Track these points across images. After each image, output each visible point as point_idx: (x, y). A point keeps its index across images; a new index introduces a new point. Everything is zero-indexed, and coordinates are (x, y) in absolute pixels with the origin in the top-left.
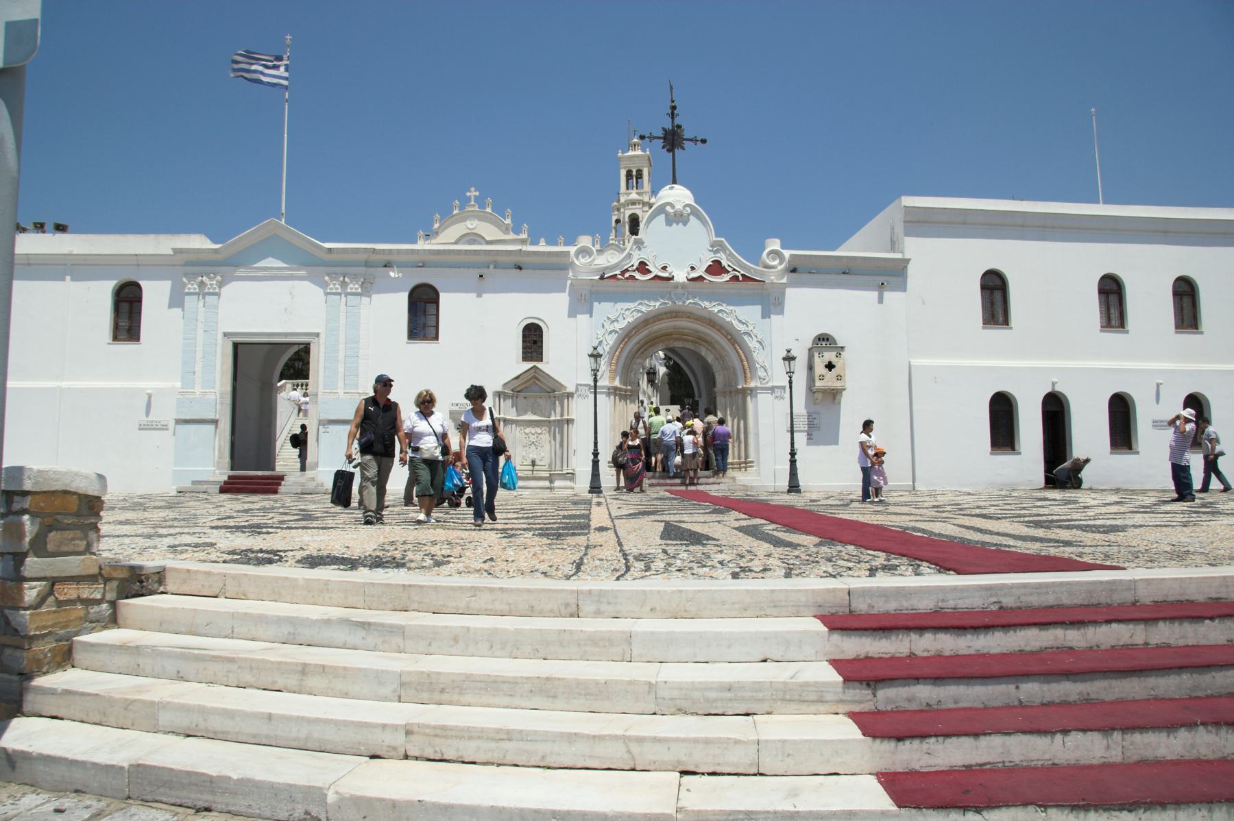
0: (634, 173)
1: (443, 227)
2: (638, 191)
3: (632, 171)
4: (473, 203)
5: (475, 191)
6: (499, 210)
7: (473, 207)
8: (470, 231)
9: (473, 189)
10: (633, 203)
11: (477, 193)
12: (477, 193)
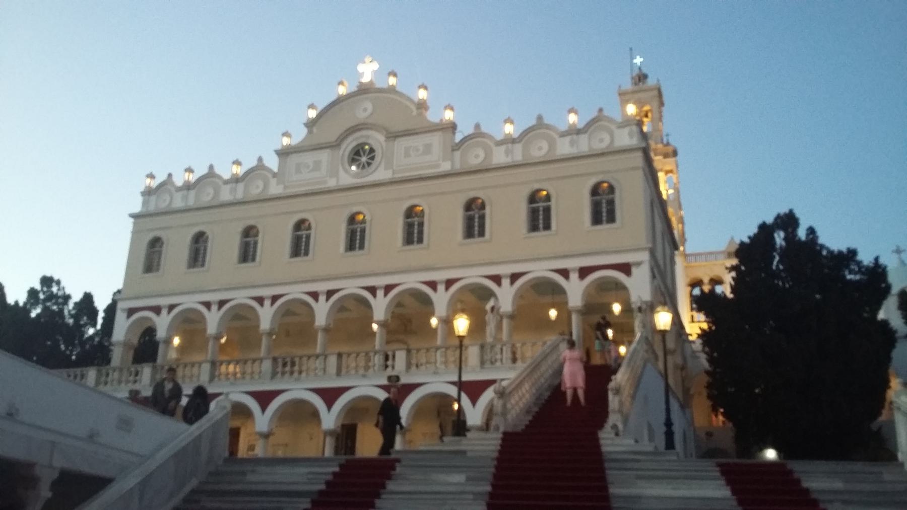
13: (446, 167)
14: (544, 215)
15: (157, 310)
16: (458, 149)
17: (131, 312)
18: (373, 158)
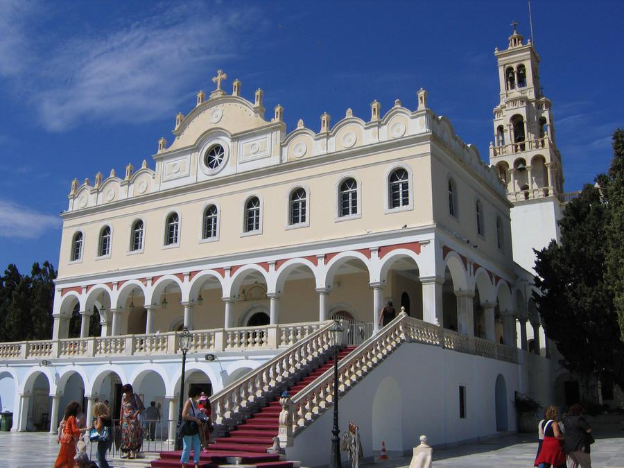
0: (515, 69)
1: (184, 126)
2: (522, 89)
3: (512, 69)
4: (218, 89)
5: (222, 74)
6: (247, 94)
7: (218, 94)
8: (214, 126)
9: (219, 72)
10: (514, 101)
11: (224, 76)
12: (224, 76)
13: (275, 161)
14: (353, 198)
15: (79, 289)
16: (286, 145)
17: (63, 291)
18: (222, 157)
